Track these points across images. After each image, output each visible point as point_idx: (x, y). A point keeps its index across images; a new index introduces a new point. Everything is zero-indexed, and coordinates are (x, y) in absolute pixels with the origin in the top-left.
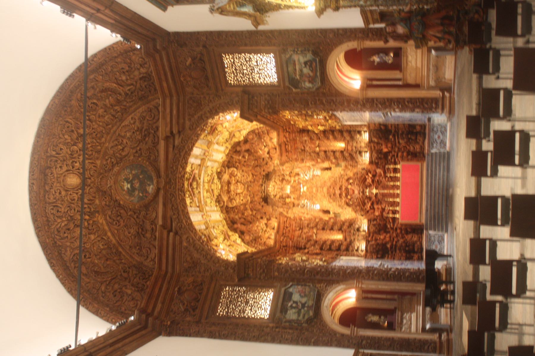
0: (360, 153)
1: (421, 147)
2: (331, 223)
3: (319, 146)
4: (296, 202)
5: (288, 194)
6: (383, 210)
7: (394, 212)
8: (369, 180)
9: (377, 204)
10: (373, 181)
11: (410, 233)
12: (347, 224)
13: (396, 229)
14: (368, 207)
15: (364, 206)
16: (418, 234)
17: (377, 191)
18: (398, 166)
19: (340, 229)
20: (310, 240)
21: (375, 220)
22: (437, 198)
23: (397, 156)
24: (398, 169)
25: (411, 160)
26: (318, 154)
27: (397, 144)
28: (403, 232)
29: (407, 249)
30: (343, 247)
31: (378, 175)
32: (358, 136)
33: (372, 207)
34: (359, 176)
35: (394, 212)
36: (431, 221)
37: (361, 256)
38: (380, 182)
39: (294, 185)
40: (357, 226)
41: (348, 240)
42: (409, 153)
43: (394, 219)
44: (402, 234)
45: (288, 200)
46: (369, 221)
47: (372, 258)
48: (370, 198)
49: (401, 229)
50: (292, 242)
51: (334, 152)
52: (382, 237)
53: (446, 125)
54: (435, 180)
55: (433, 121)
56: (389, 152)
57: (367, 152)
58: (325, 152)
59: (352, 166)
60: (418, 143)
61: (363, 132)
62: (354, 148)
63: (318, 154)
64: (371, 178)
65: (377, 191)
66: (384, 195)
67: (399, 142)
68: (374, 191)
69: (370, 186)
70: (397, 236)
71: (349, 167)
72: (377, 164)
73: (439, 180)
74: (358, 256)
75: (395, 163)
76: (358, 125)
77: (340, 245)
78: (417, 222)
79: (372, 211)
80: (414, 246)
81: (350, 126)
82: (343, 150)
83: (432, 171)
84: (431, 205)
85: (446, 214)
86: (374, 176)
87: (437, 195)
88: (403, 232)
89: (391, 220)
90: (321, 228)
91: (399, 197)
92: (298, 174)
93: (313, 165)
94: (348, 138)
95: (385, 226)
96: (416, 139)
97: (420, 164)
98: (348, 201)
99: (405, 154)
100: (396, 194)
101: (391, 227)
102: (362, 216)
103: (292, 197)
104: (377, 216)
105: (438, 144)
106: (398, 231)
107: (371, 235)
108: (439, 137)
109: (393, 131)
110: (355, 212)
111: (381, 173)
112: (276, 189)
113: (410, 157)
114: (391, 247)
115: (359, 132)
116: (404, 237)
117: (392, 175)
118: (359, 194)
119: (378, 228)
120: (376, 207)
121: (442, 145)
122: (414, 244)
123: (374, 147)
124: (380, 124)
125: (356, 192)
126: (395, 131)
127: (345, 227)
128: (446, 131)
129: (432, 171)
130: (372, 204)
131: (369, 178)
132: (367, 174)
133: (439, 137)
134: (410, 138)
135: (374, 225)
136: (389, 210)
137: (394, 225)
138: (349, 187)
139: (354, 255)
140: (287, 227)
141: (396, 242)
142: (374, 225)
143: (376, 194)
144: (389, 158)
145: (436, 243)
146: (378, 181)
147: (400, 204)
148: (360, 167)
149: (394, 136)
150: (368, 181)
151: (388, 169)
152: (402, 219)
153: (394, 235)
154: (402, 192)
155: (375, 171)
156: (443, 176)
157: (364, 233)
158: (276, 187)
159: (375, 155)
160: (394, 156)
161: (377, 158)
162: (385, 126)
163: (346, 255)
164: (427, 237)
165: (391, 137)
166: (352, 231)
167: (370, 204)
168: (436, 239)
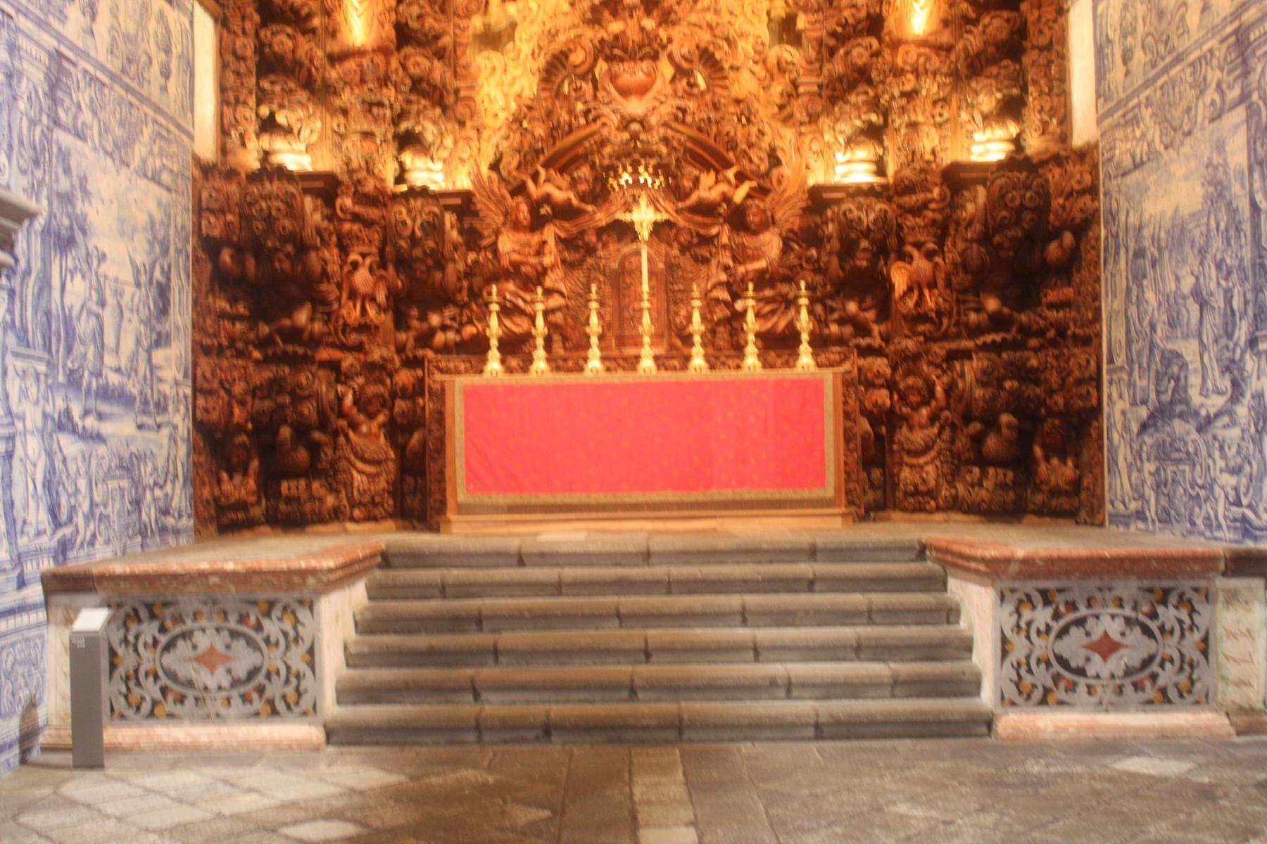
0: (874, 133)
1: (932, 494)
6: (532, 280)
7: (515, 347)
8: (709, 188)
9: (566, 243)
10: (706, 209)
11: (401, 449)
12: (439, 71)
13: (414, 363)
14: (549, 188)
15: (546, 166)
16: (397, 491)
17: (645, 234)
18: (806, 357)
19: (404, 35)
21: (472, 238)
22: (611, 634)
23: (865, 352)
24: (795, 355)
25: (848, 437)
27: (939, 349)
28: (401, 405)
29: (285, 432)
30: (283, 41)
31: (748, 240)
32: (987, 102)
33: (546, 210)
34: (732, 127)
35: (515, 347)
36: (443, 590)
37: (223, 150)
38: (704, 252)
40: (430, 132)
41: (333, 74)
42: (886, 420)
43: (477, 347)
44: (386, 403)
46: (464, 204)
47: (199, 210)
48: (599, 194)
49: (419, 388)
52: (362, 278)
53: (1204, 701)
54: (744, 617)
55: (1232, 597)
56: (885, 306)
57: (880, 170)
59: (794, 90)
60: (953, 476)
61: (1013, 129)
62: (909, 83)
64: (726, 199)
65: (645, 234)
66: (621, 281)
67: (952, 356)
68: (644, 216)
69: (676, 192)
70: (376, 370)
71: (777, 88)
72: (807, 236)
73: (756, 651)
74: (223, 131)
75: (820, 342)
76: (1065, 94)
77: (298, 21)
78: (460, 490)
79: (524, 213)
80: (311, 471)
81: (1056, 50)
82: (890, 24)
83: (810, 585)
84: (558, 588)
85: (480, 727)
86: (738, 219)
87: (634, 636)
88: (401, 405)
89: (469, 330)
91: (608, 369)
94: (973, 41)
95: (442, 298)
96: (983, 462)
97: (829, 492)
98: (577, 57)
99: (882, 397)
100: (630, 351)
101: (432, 332)
102: (495, 167)
104: (494, 247)
105: (1042, 646)
106: (405, 377)
107: (373, 213)
108: (1107, 647)
109: (1023, 318)
110: (517, 120)
111: (756, 258)
113: (865, 425)
114: (294, 335)
115: (1011, 108)
116: (371, 416)
117: (751, 324)
118: (625, 123)
119: (418, 252)
120: (550, 233)
121: (1042, 677)
122: (333, 476)
123: (917, 211)
124: (1084, 227)
125: (635, 107)
126: (1026, 331)
127: (419, 62)
128: (1164, 699)
129: (810, 585)
130: (565, 212)
131: (723, 187)
132: (741, 177)
133: (1107, 647)
134: (990, 422)
135: (434, 227)
136: (532, 319)
137: (446, 349)
138: (666, 70)
139: (227, 97)
141: (334, 366)
142: (434, 227)
143: (625, 231)
144: (852, 307)
145: (244, 658)
146: (707, 241)
147: (573, 378)
148: (786, 138)
149: (997, 322)
150: (707, 179)
151: (790, 303)
152: (470, 393)
153: (376, 354)
154: (648, 386)
155: (768, 222)
156: (790, 688)
157: (389, 171)
159: (869, 214)
160: (863, 330)
161: (847, 225)
162: (1069, 266)
163: (226, 57)
164: (291, 586)
165: (992, 304)
166: (389, 94)
167: (559, 195)
168: (274, 659)
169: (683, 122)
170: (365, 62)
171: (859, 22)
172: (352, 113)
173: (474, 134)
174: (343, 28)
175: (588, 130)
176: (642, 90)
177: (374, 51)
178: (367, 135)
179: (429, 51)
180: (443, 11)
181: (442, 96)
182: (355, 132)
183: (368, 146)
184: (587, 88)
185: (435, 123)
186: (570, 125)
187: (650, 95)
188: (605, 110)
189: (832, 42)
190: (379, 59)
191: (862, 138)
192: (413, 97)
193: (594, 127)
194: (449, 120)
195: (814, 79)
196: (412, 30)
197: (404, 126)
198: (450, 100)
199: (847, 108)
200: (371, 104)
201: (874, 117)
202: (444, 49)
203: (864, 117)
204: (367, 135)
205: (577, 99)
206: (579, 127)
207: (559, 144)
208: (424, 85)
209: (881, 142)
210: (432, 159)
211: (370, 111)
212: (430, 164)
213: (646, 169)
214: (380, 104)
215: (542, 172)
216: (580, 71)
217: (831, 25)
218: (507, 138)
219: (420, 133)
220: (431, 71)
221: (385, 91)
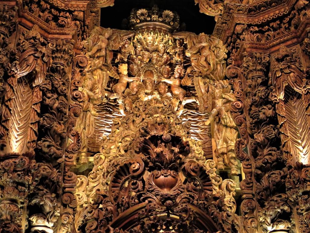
2: (59, 128)
3: (290, 94)
4: (120, 87)
5: (139, 76)
12: (55, 174)
20: (12, 60)
26: (266, 101)
39: (162, 87)
45: (124, 69)
50: (13, 8)
51: (276, 142)
58: (273, 120)
63: (266, 101)
90: (48, 101)
92: (189, 91)
93: (219, 114)
103: (131, 80)
112: (147, 53)
127: (45, 169)
138: (182, 177)
140: (56, 18)
158: (155, 55)
169: (193, 204)
170: (17, 161)
171: (273, 162)
172: (6, 189)
173: (70, 211)
174: (7, 145)
175: (141, 205)
176: (171, 186)
177: (23, 155)
178: (13, 202)
179: (51, 165)
180: (61, 145)
181: (56, 188)
182: (6, 200)
183: (12, 207)
184: (140, 183)
185: (52, 201)
186: (128, 204)
187: (174, 188)
188: (149, 195)
189: (259, 172)
190: (26, 160)
191: (280, 220)
192: (41, 187)
193: (143, 204)
194: (58, 201)
195: (250, 191)
196: (45, 153)
197: (34, 201)
198: (60, 192)
199: (273, 203)
200: (18, 184)
201: (286, 208)
202: (59, 164)
203: (281, 208)
204: (13, 202)
205: (134, 189)
206: (136, 204)
207: (121, 215)
208: (47, 181)
209: (290, 221)
210: (48, 221)
211: (17, 188)
212: (46, 224)
213: (174, 229)
214: (23, 185)
215: (111, 229)
216: (136, 174)
217: (260, 163)
218: (90, 212)
219: (42, 205)
220: (52, 173)
221: (27, 177)
